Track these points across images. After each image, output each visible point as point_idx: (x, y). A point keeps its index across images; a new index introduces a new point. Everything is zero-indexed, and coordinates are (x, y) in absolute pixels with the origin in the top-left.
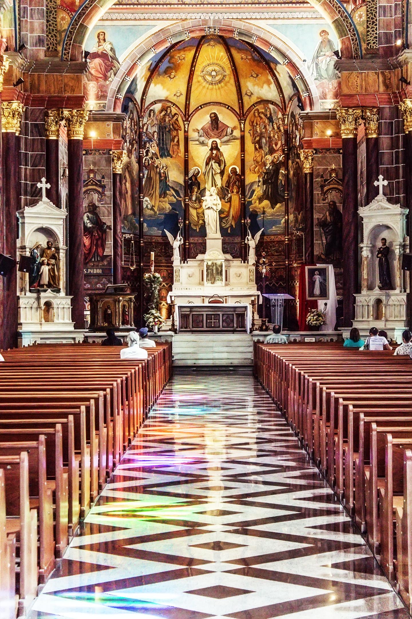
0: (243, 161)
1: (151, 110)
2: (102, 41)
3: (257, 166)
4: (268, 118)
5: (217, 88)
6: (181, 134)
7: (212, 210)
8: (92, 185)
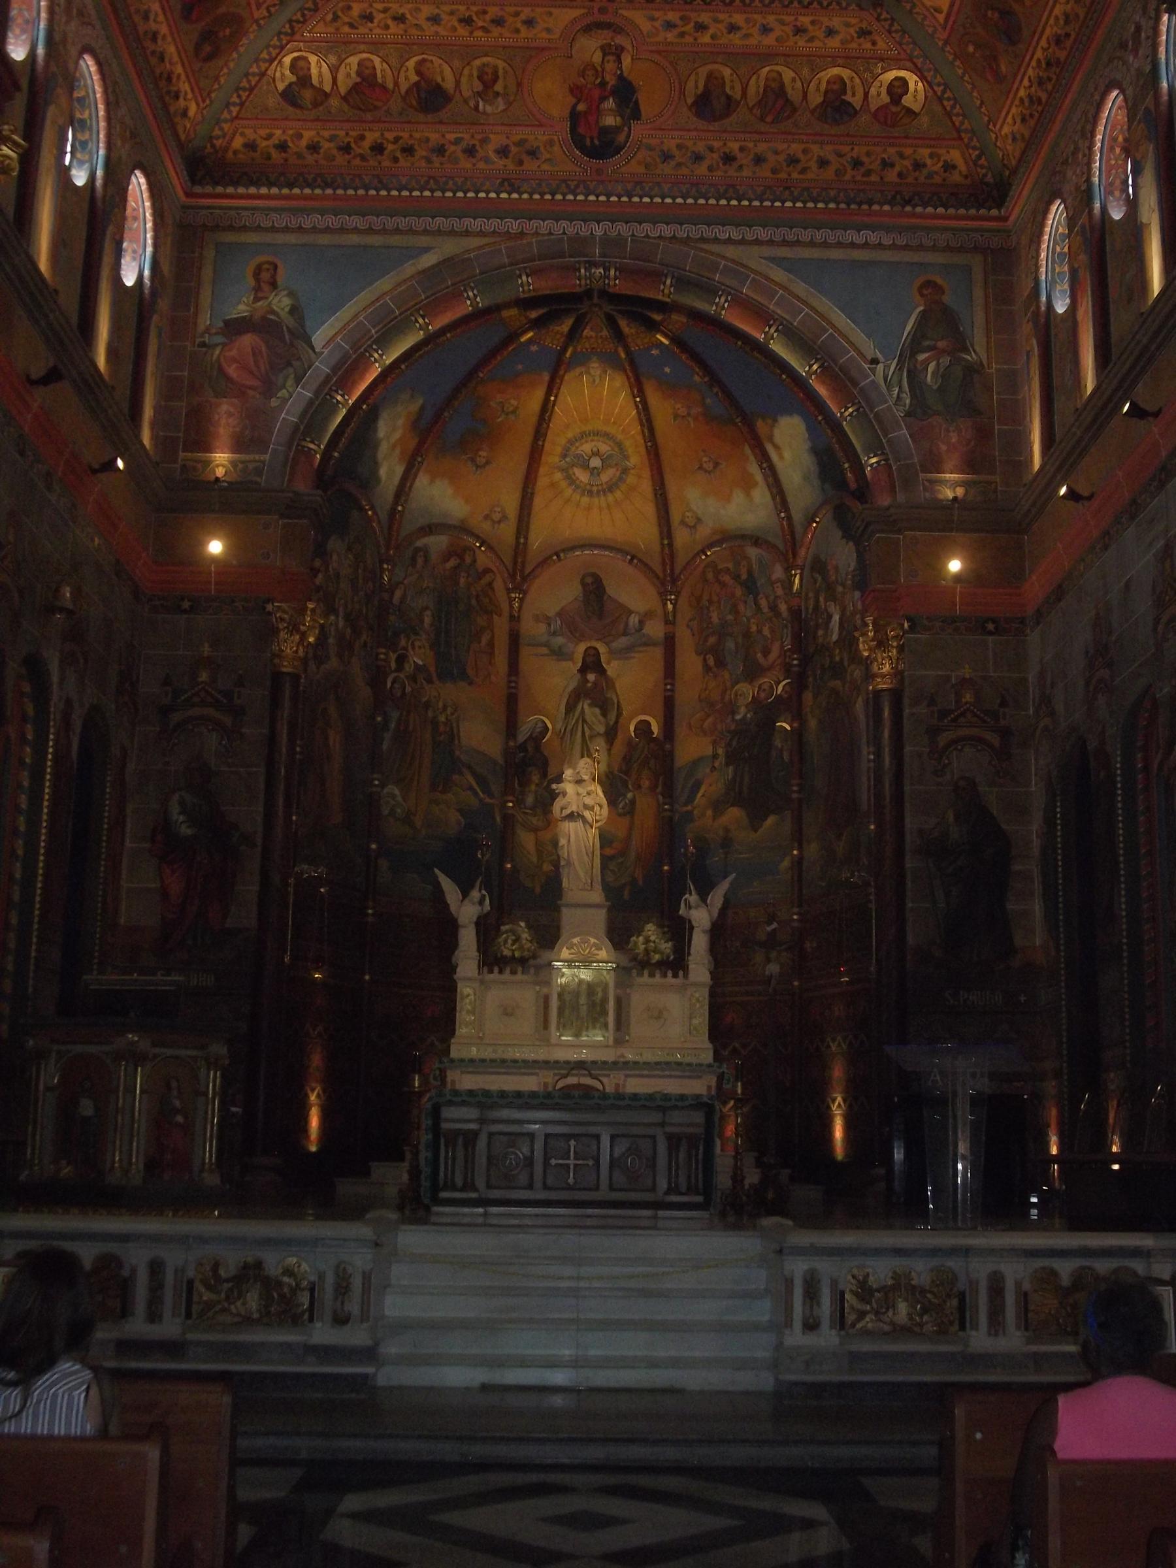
0: (669, 704)
1: (417, 550)
2: (266, 287)
3: (708, 716)
5: (604, 505)
6: (501, 625)
7: (580, 824)
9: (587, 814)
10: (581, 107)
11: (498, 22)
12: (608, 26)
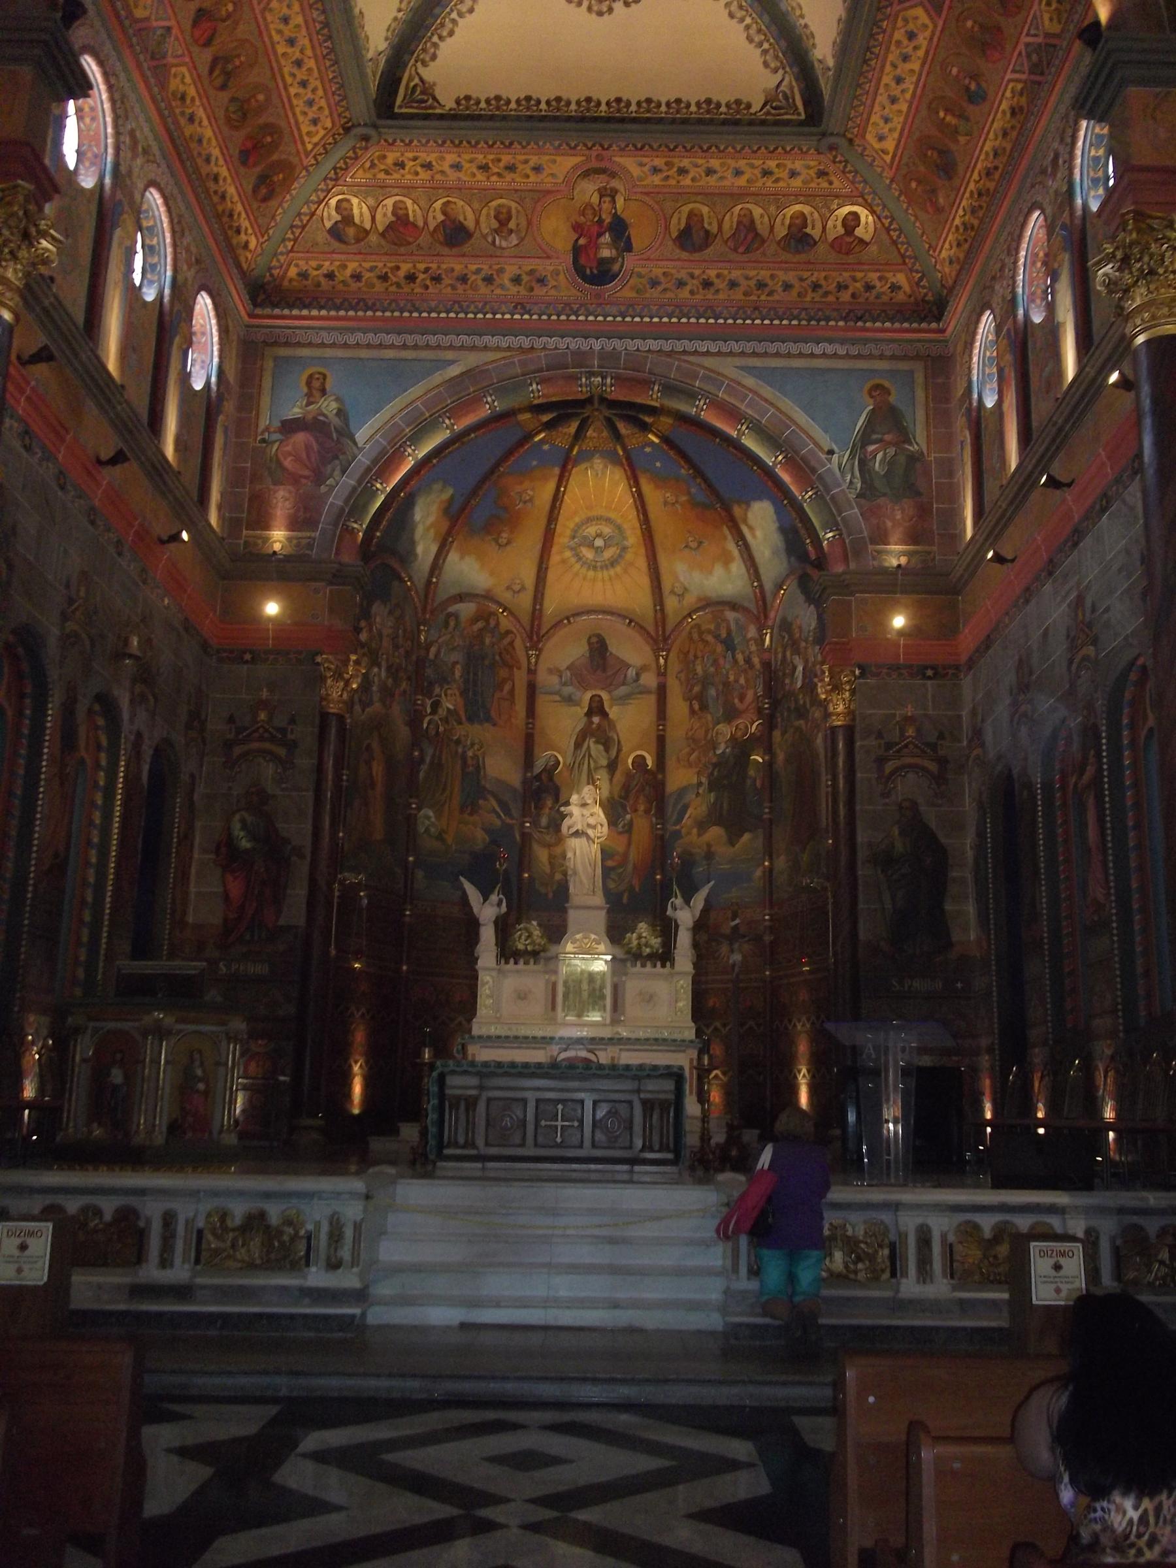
0: (661, 741)
1: (449, 615)
2: (317, 394)
3: (693, 750)
4: (724, 642)
5: (606, 578)
6: (520, 679)
7: (584, 840)
8: (261, 739)
9: (590, 832)
10: (582, 241)
11: (511, 168)
12: (602, 171)
